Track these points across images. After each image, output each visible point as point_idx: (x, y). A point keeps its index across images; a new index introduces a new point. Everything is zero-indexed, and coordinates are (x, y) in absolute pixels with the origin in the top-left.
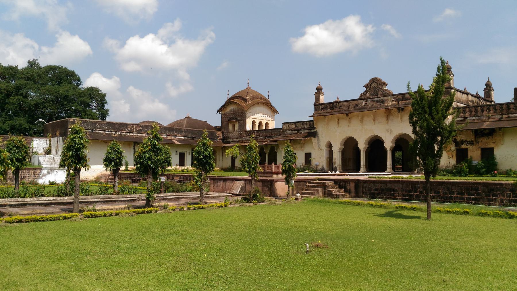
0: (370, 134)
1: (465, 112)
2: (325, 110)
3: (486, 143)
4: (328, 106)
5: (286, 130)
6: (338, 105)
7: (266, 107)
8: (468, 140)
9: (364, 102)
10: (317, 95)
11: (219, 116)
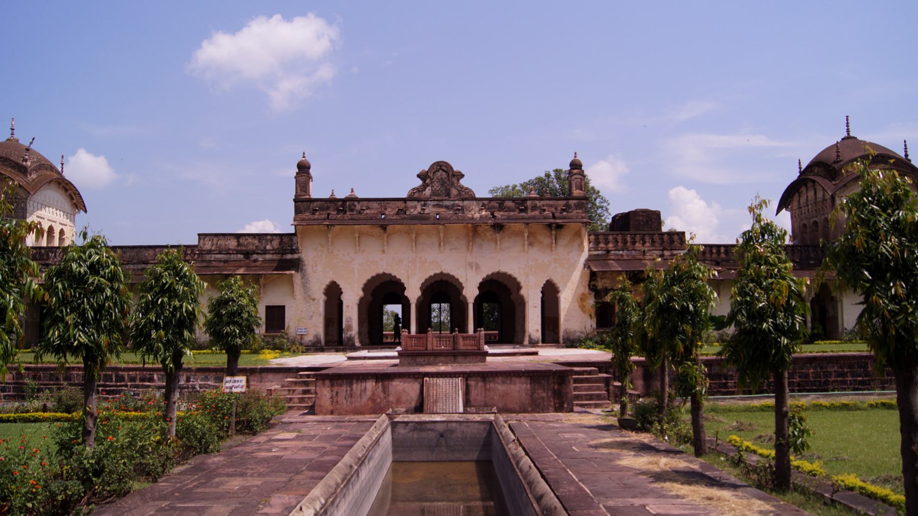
0: (488, 269)
1: (607, 243)
2: (325, 215)
4: (332, 205)
5: (210, 252)
6: (358, 207)
7: (62, 192)
9: (419, 209)
10: (303, 179)
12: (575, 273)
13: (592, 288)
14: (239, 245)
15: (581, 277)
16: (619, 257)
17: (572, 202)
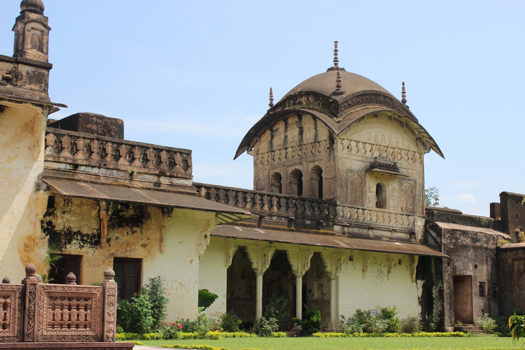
1: (74, 150)
3: (126, 243)
8: (85, 231)
12: (18, 198)
13: (48, 228)
15: (29, 205)
16: (93, 178)
17: (23, 69)
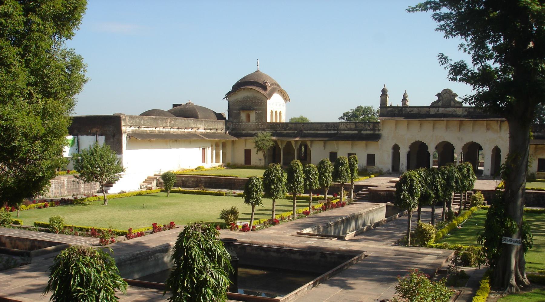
10: (383, 97)
11: (226, 103)
14: (356, 127)
